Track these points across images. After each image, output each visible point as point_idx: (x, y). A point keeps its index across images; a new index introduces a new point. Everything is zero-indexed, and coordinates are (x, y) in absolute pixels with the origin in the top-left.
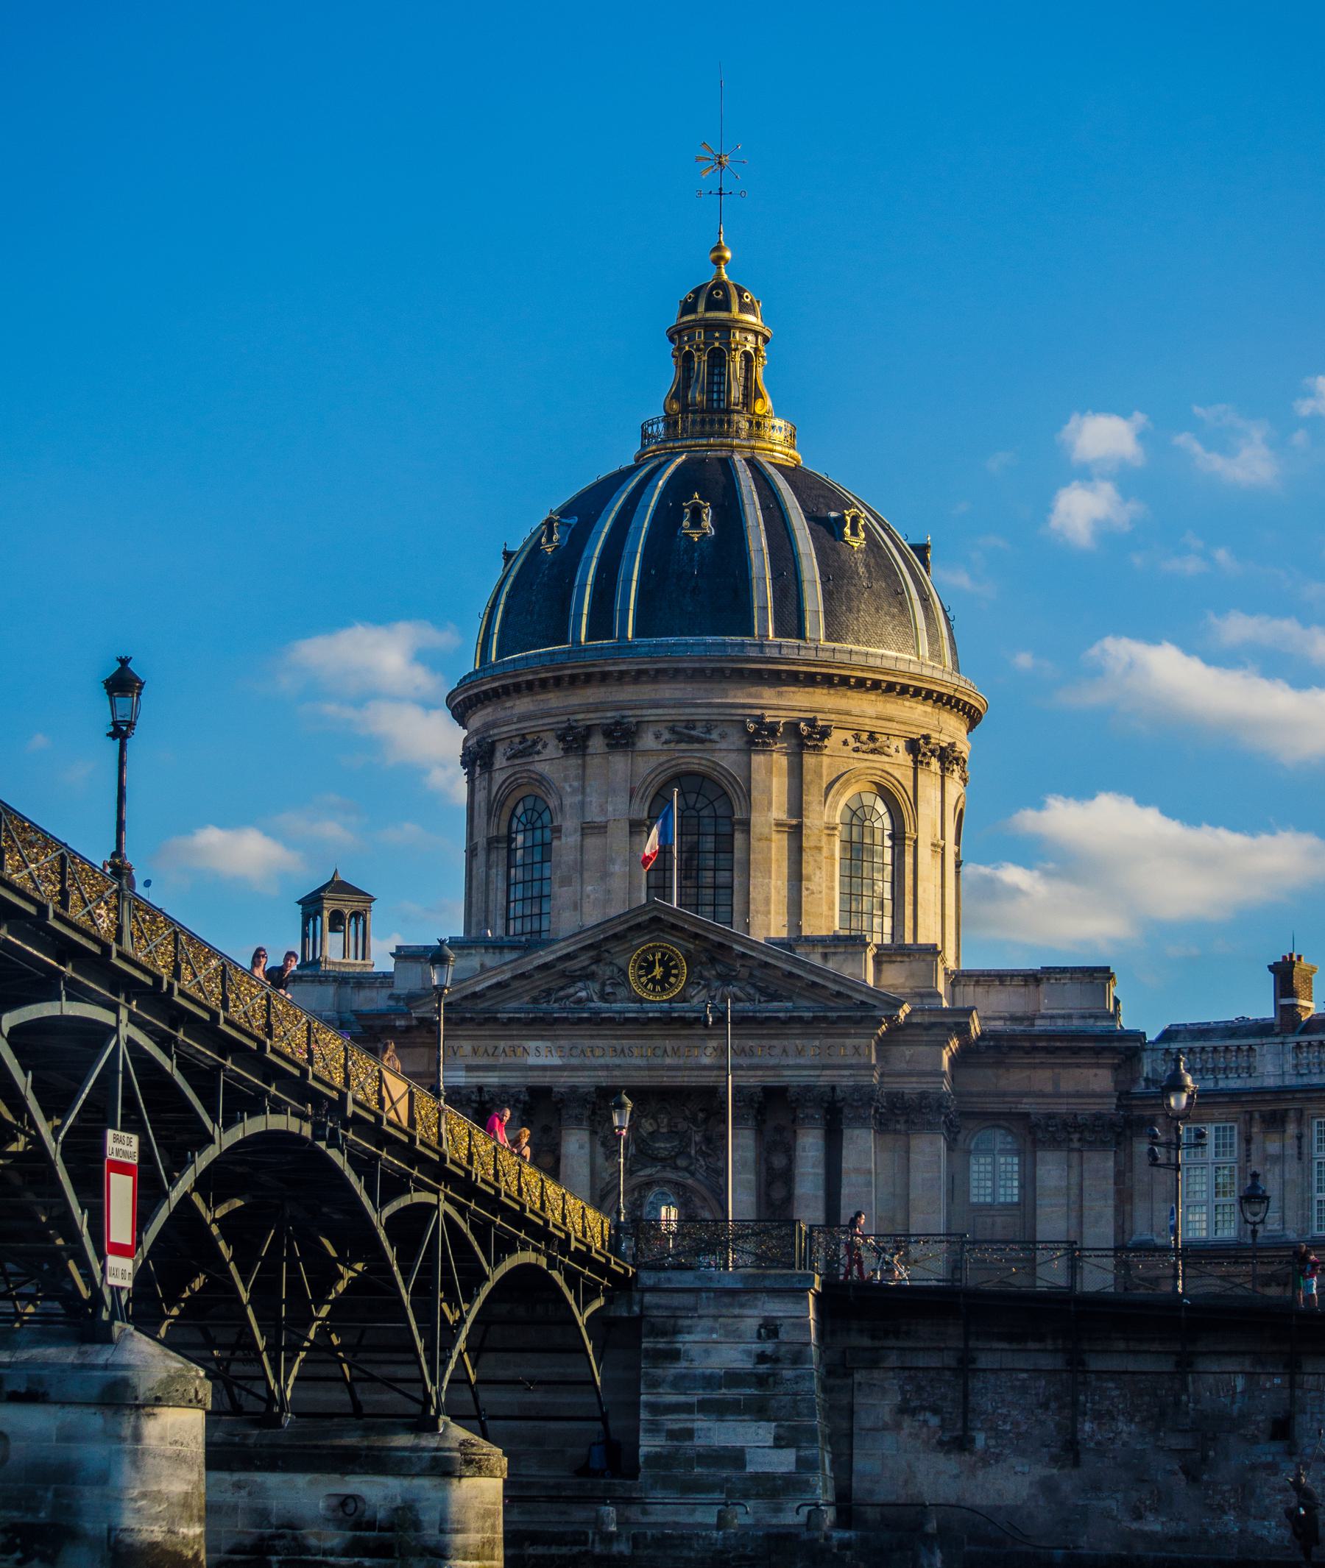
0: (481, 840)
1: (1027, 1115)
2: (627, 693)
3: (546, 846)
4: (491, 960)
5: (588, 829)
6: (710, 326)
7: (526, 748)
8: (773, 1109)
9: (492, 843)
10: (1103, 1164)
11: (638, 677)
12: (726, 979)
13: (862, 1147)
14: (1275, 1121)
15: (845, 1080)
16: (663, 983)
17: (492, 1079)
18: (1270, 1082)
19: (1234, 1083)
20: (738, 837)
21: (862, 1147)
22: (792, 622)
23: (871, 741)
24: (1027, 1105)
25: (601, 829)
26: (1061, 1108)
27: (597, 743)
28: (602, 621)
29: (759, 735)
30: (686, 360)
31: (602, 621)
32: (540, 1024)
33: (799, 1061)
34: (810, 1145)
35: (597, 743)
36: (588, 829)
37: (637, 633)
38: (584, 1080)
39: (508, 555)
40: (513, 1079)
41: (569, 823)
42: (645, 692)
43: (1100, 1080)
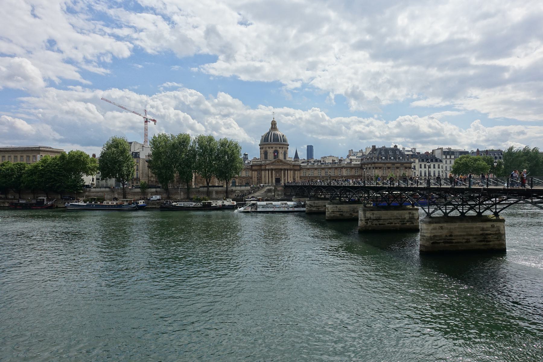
7: (266, 148)
8: (285, 170)
13: (289, 172)
29: (280, 148)
30: (272, 125)
33: (286, 167)
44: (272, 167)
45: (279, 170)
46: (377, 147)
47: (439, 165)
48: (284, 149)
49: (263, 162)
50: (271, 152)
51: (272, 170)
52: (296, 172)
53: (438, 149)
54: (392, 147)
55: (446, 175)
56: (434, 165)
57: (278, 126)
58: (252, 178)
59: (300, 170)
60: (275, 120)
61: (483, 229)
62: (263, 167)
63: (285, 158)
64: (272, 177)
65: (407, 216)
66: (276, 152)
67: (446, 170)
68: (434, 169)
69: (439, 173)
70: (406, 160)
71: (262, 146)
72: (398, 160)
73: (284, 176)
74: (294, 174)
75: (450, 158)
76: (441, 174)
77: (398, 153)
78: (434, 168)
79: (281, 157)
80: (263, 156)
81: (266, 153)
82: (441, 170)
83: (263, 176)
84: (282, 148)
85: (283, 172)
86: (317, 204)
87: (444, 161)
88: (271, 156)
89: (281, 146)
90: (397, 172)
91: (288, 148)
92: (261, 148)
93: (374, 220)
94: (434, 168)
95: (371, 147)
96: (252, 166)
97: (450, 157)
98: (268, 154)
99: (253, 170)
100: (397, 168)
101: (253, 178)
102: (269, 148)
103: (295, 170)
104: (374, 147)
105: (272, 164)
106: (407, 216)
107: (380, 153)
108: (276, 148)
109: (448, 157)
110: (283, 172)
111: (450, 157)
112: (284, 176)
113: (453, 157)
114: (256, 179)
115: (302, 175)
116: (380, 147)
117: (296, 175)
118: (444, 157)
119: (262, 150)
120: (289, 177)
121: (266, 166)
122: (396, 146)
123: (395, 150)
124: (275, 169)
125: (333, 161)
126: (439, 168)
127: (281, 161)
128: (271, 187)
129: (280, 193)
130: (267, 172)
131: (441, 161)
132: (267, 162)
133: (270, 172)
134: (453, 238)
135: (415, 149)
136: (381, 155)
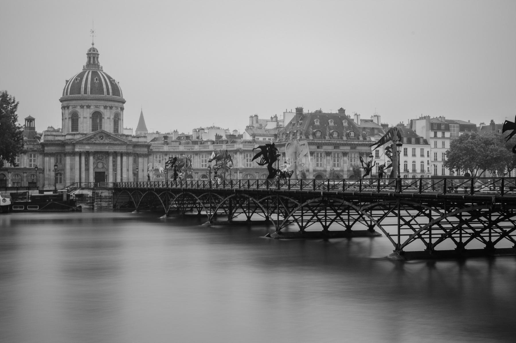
0: (68, 118)
1: (137, 154)
2: (89, 102)
3: (77, 120)
4: (81, 136)
5: (84, 118)
6: (93, 54)
7: (75, 107)
8: (115, 154)
9: (69, 118)
10: (146, 159)
11: (91, 100)
12: (110, 139)
13: (125, 158)
15: (123, 151)
16: (102, 139)
17: (82, 150)
18: (166, 150)
19: (161, 150)
20: (103, 120)
23: (117, 107)
24: (137, 152)
25: (86, 118)
26: (141, 153)
27: (85, 107)
28: (85, 92)
29: (105, 107)
30: (89, 58)
31: (85, 92)
32: (88, 144)
33: (118, 149)
34: (119, 158)
35: (85, 107)
36: (84, 118)
37: (91, 94)
38: (93, 150)
39: (67, 81)
40: (84, 150)
41: (82, 117)
42: (92, 102)
44: (87, 148)
46: (305, 111)
47: (422, 150)
48: (114, 110)
49: (68, 137)
51: (87, 154)
52: (140, 160)
53: (421, 118)
54: (335, 111)
55: (436, 170)
56: (414, 150)
57: (102, 61)
58: (43, 171)
59: (147, 156)
60: (95, 46)
62: (68, 149)
63: (116, 130)
64: (87, 170)
66: (97, 117)
67: (436, 160)
68: (414, 159)
69: (422, 166)
70: (361, 138)
71: (65, 103)
72: (345, 138)
73: (115, 170)
74: (135, 162)
75: (443, 137)
76: (426, 169)
77: (345, 124)
78: (414, 155)
79: (108, 126)
80: (69, 123)
81: (75, 119)
82: (425, 159)
83: (68, 167)
84: (111, 108)
85: (111, 158)
87: (432, 142)
88: (85, 126)
90: (345, 162)
91: (122, 109)
92: (63, 108)
94: (414, 155)
95: (294, 111)
96: (43, 145)
97: (443, 133)
98: (80, 120)
99: (46, 155)
100: (345, 154)
101: (47, 172)
102: (82, 107)
103: (137, 156)
104: (299, 111)
105: (88, 140)
107: (312, 123)
108: (96, 107)
109: (439, 134)
110: (111, 158)
111: (443, 133)
112: (115, 170)
113: (447, 134)
114: (53, 174)
116: (313, 110)
117: (140, 167)
118: (432, 134)
119: (67, 112)
120: (124, 170)
121: (74, 145)
122: (342, 110)
123: (340, 117)
124: (95, 153)
125: (218, 137)
126: (422, 156)
127: (108, 135)
128: (85, 192)
129: (104, 204)
130: (77, 158)
131: (426, 142)
132: (77, 137)
135: (378, 117)
136: (314, 127)
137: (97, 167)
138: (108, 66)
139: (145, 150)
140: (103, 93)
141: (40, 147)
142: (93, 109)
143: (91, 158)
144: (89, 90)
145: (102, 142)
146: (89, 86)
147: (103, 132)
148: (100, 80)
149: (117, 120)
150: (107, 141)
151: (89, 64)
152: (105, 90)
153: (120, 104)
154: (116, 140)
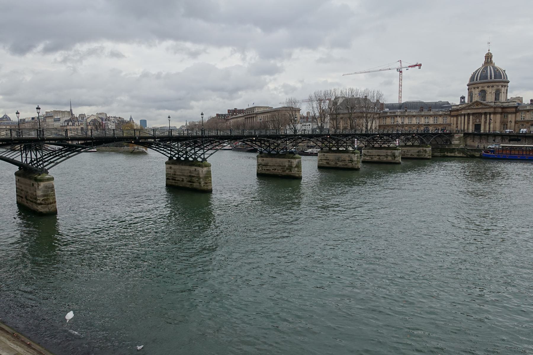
7: (471, 89)
8: (485, 114)
10: (514, 115)
13: (492, 116)
14: (528, 112)
21: (492, 116)
22: (491, 78)
28: (477, 80)
29: (488, 87)
33: (487, 111)
34: (488, 116)
43: (514, 110)
44: (469, 111)
45: (478, 115)
48: (495, 88)
50: (476, 92)
51: (469, 115)
52: (510, 116)
61: (190, 172)
64: (468, 123)
65: (287, 164)
66: (483, 93)
73: (485, 123)
79: (490, 98)
84: (493, 86)
85: (483, 116)
86: (370, 152)
89: (492, 84)
93: (263, 165)
96: (451, 111)
98: (474, 96)
102: (474, 88)
106: (287, 164)
110: (483, 116)
115: (519, 119)
117: (509, 120)
124: (473, 114)
130: (463, 117)
133: (466, 117)
134: (176, 176)
137: (476, 122)
138: (498, 62)
139: (514, 110)
140: (487, 78)
141: (449, 112)
142: (480, 89)
143: (471, 117)
144: (479, 78)
145: (477, 107)
146: (479, 76)
147: (477, 102)
148: (487, 71)
149: (497, 94)
150: (480, 107)
151: (485, 63)
152: (489, 76)
153: (502, 84)
154: (485, 105)
